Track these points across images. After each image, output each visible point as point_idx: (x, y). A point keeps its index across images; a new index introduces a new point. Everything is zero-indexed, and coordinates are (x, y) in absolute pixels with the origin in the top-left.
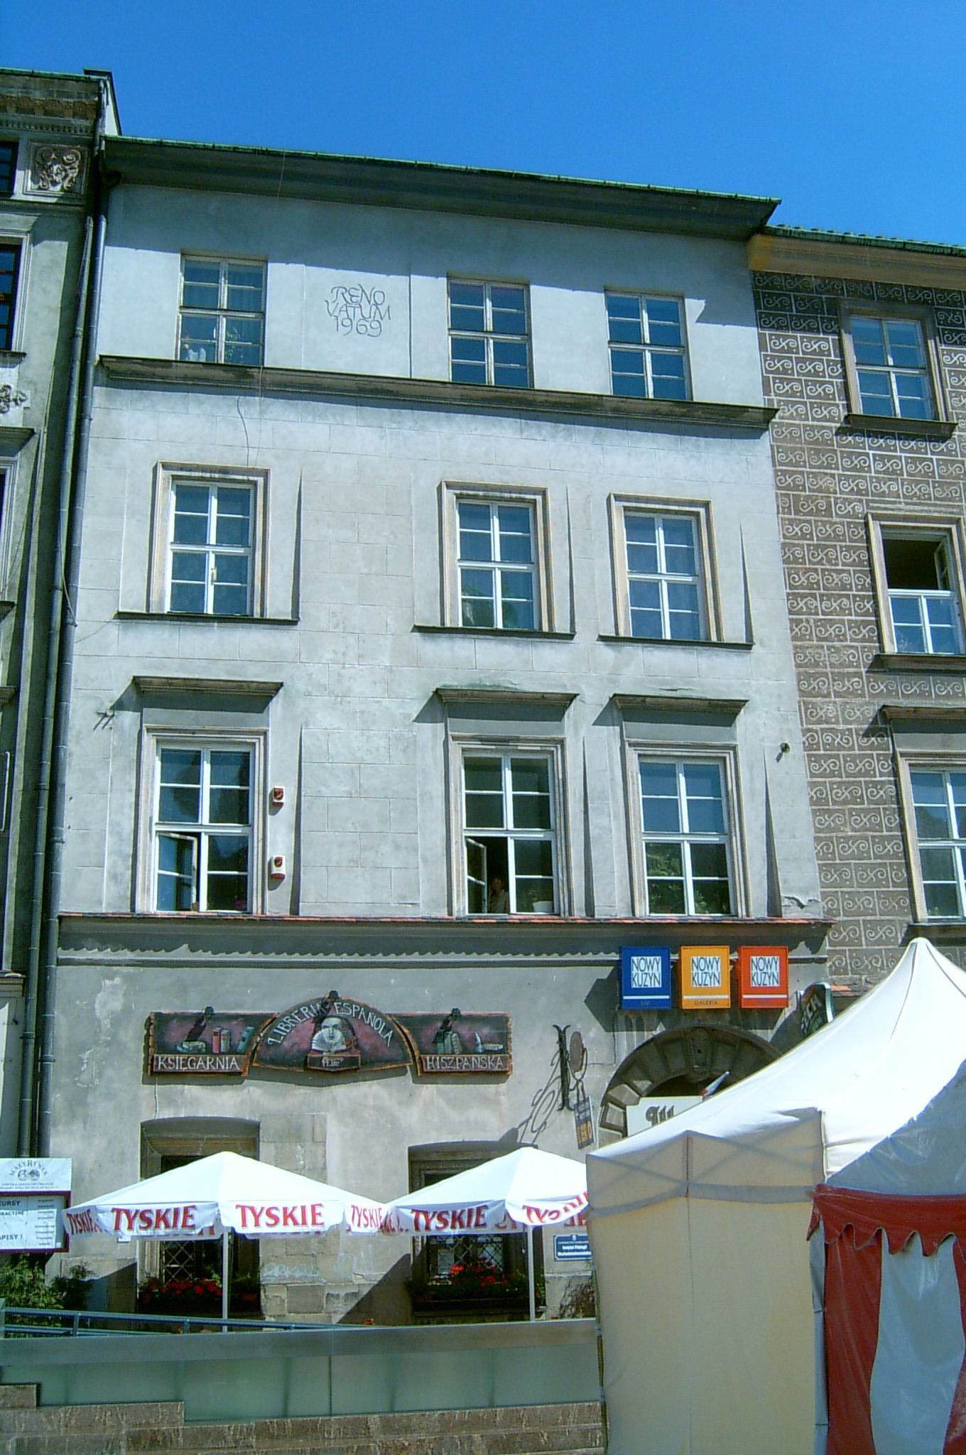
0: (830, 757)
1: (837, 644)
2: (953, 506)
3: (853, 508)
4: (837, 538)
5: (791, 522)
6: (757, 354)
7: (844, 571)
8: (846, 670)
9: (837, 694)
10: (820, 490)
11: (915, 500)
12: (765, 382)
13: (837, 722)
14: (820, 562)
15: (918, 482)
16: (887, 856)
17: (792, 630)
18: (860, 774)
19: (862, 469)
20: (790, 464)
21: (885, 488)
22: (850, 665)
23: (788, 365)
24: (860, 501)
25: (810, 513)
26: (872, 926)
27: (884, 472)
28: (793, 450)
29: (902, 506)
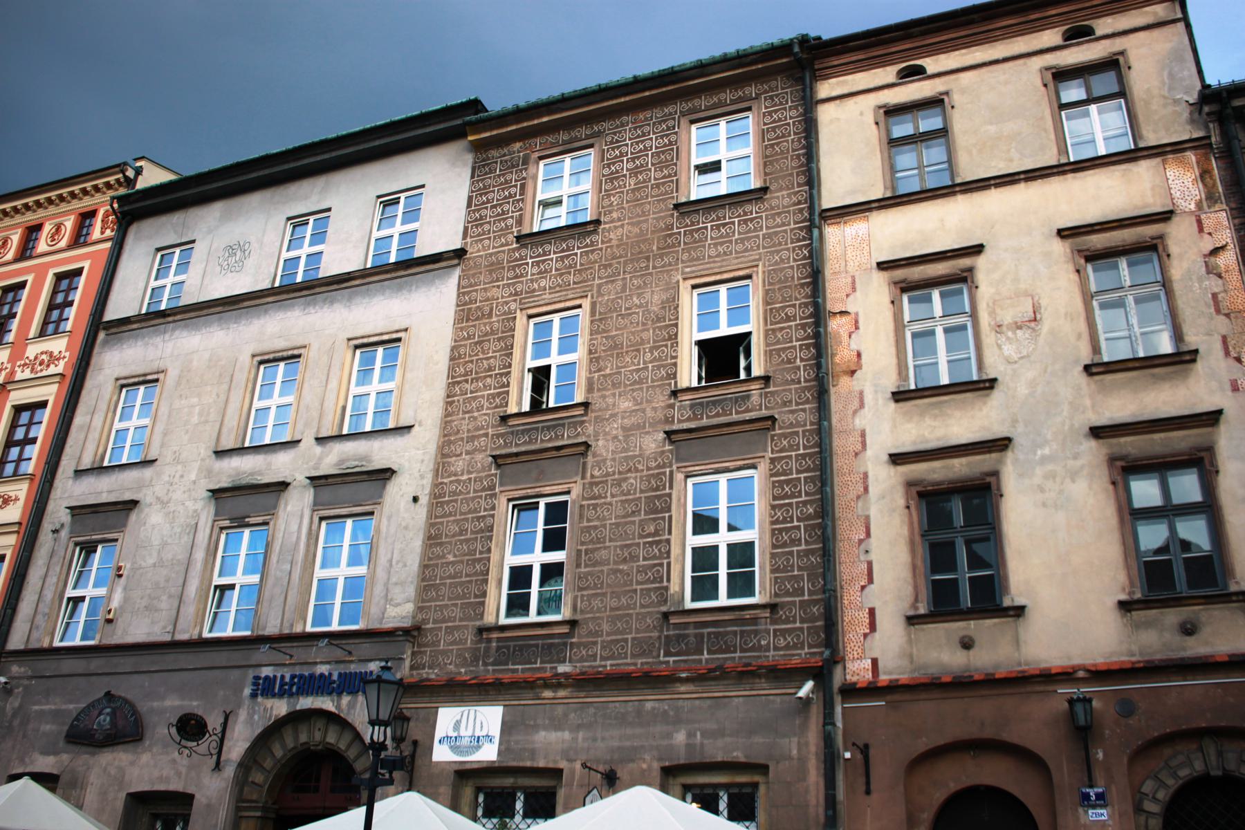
1: (476, 414)
4: (493, 332)
5: (462, 329)
6: (464, 211)
9: (468, 453)
12: (466, 229)
13: (462, 474)
14: (477, 355)
16: (476, 574)
18: (470, 512)
19: (522, 276)
20: (471, 286)
21: (536, 286)
23: (483, 212)
24: (515, 301)
25: (477, 319)
26: (450, 630)
28: (474, 275)
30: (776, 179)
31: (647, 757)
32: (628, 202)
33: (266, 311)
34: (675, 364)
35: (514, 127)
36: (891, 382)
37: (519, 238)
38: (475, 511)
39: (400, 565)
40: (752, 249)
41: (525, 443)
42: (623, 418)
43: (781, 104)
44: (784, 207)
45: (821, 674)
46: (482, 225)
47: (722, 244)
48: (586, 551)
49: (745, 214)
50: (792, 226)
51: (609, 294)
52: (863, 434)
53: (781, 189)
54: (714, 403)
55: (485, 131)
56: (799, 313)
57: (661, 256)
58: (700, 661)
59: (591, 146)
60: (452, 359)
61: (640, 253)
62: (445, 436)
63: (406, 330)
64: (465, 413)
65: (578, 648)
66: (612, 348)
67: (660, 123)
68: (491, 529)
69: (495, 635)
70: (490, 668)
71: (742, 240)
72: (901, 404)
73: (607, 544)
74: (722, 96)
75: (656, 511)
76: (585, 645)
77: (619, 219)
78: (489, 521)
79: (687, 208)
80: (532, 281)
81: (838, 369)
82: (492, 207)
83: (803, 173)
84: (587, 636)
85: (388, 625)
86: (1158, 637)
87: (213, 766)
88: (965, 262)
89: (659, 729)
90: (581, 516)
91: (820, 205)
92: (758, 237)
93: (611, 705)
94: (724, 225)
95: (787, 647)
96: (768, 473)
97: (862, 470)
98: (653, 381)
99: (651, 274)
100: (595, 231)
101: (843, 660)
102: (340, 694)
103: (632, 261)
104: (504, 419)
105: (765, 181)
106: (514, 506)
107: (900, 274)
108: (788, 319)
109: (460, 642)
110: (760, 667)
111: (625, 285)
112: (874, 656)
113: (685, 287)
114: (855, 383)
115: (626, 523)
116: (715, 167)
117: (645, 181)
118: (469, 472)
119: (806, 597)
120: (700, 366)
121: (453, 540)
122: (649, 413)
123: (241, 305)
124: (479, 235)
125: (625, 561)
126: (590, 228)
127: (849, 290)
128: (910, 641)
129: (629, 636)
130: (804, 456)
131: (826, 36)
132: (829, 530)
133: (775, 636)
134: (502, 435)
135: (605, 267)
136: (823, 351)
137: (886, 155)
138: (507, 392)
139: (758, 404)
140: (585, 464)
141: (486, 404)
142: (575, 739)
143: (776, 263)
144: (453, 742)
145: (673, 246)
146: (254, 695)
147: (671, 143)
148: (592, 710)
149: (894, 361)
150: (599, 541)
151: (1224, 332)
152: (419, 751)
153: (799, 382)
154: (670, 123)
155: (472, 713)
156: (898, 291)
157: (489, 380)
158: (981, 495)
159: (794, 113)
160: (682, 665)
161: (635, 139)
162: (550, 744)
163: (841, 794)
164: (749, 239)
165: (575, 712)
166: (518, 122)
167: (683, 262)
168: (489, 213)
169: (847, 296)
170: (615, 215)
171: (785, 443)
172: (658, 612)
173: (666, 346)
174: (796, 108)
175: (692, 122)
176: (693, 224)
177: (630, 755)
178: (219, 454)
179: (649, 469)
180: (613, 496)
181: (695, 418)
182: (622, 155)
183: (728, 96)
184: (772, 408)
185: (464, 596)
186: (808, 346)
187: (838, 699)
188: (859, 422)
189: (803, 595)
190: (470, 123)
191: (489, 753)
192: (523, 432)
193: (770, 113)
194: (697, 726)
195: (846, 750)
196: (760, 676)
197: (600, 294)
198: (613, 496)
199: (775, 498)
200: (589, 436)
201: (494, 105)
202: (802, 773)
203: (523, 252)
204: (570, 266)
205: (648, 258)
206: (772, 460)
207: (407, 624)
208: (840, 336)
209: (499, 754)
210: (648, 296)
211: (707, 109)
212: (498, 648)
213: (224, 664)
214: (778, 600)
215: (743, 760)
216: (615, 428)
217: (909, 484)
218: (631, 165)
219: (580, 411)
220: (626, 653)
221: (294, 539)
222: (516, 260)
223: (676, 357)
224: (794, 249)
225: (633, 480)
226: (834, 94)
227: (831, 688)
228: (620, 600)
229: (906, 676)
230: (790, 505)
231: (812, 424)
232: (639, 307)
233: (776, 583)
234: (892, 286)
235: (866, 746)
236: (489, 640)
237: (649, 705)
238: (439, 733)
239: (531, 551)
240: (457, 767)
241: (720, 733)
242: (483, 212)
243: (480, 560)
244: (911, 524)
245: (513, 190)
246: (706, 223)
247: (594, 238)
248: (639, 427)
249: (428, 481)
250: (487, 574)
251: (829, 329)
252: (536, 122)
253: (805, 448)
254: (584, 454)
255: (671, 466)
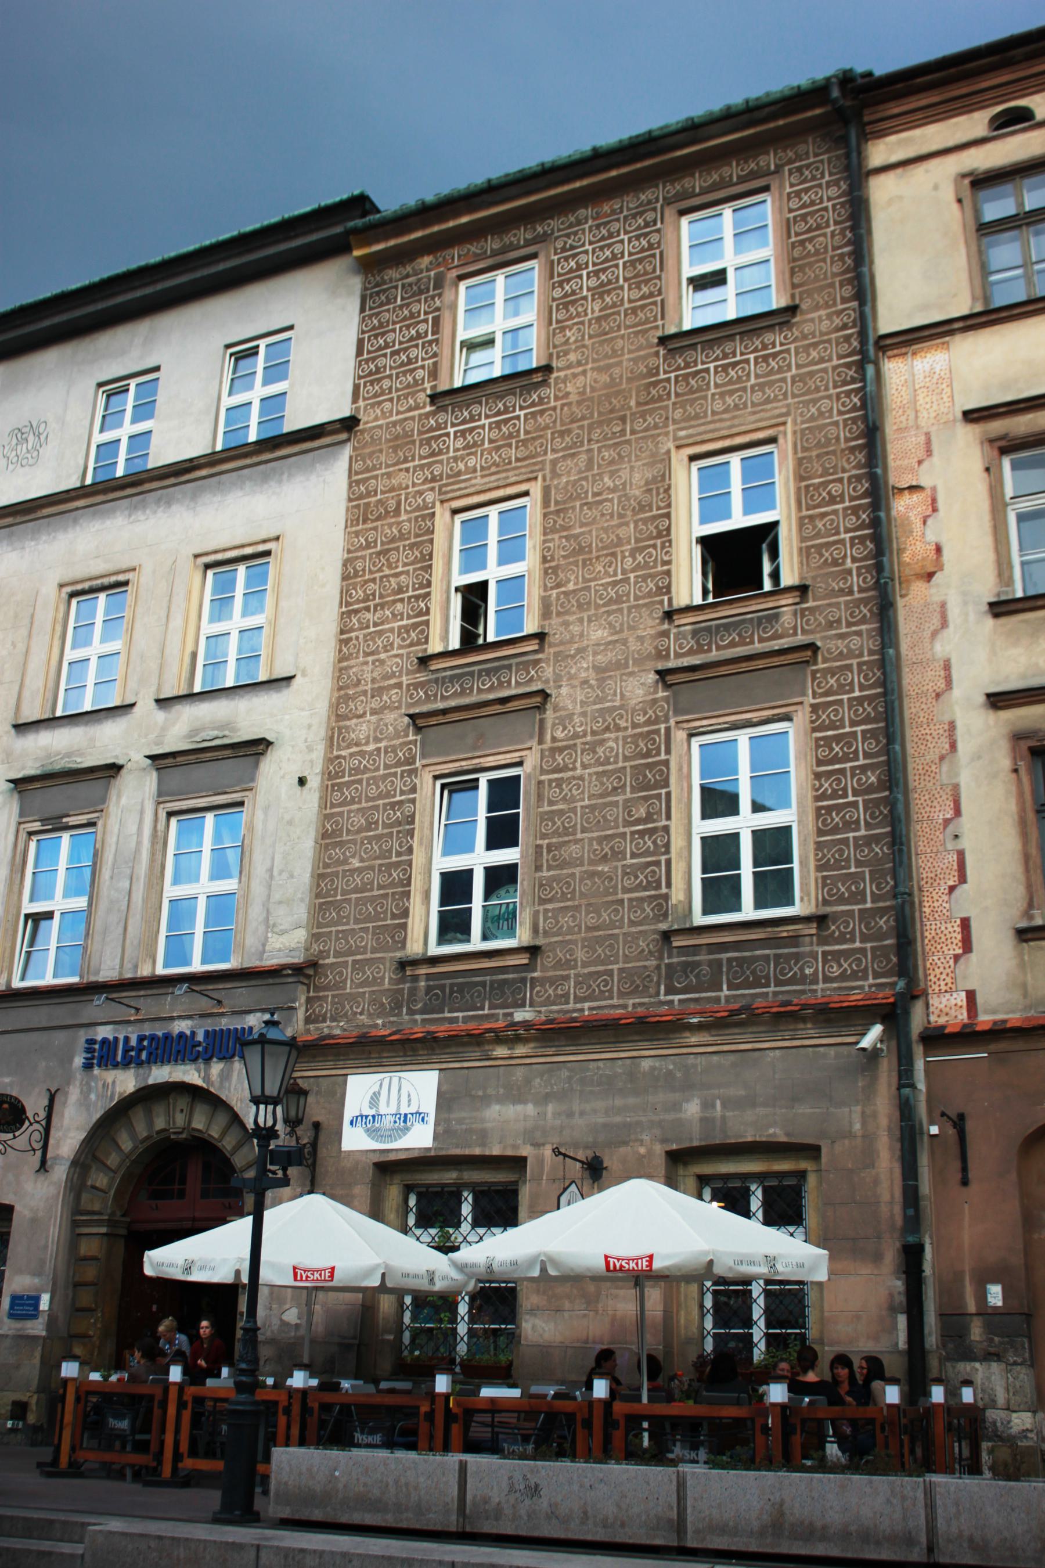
0: (353, 782)
1: (383, 656)
2: (534, 464)
3: (424, 500)
4: (402, 537)
5: (357, 534)
7: (401, 573)
8: (387, 683)
9: (374, 712)
10: (392, 489)
11: (493, 469)
12: (356, 388)
13: (367, 743)
14: (380, 570)
15: (498, 449)
16: (392, 885)
17: (340, 651)
18: (380, 796)
19: (440, 452)
20: (368, 470)
21: (461, 466)
22: (393, 675)
23: (381, 362)
24: (432, 489)
25: (378, 519)
27: (464, 448)
29: (478, 481)
30: (809, 293)
31: (646, 1138)
32: (590, 337)
33: (75, 521)
34: (668, 573)
35: (419, 234)
36: (987, 589)
37: (434, 398)
38: (388, 795)
39: (285, 875)
40: (776, 399)
41: (455, 693)
42: (595, 654)
43: (814, 178)
44: (822, 334)
45: (893, 1015)
46: (379, 380)
47: (731, 393)
48: (549, 846)
49: (765, 347)
50: (835, 362)
51: (569, 473)
52: (947, 666)
53: (817, 308)
54: (726, 627)
55: (378, 241)
56: (848, 490)
57: (643, 415)
58: (718, 1000)
59: (534, 256)
60: (345, 578)
61: (612, 411)
62: (340, 689)
63: (277, 538)
64: (367, 654)
65: (542, 985)
66: (574, 553)
67: (634, 216)
68: (411, 819)
69: (423, 971)
70: (418, 1017)
71: (761, 387)
72: (1003, 620)
73: (579, 836)
74: (726, 171)
75: (647, 787)
76: (553, 981)
77: (579, 363)
78: (408, 808)
79: (678, 343)
80: (456, 459)
81: (908, 571)
82: (393, 354)
83: (849, 281)
84: (554, 968)
85: (271, 961)
87: (37, 1165)
89: (661, 1097)
90: (540, 797)
91: (875, 329)
92: (784, 380)
93: (592, 1065)
94: (734, 365)
95: (843, 977)
96: (809, 726)
97: (947, 718)
98: (637, 598)
99: (628, 442)
100: (544, 383)
101: (925, 993)
102: (208, 1060)
103: (600, 423)
104: (424, 661)
105: (793, 296)
106: (443, 787)
107: (997, 427)
108: (833, 500)
109: (375, 981)
110: (805, 1006)
111: (590, 460)
112: (970, 988)
113: (679, 459)
114: (933, 591)
115: (606, 805)
116: (717, 278)
117: (614, 305)
118: (377, 740)
119: (869, 905)
120: (704, 574)
121: (358, 837)
122: (633, 645)
123: (39, 514)
124: (375, 396)
125: (604, 859)
126: (538, 378)
127: (921, 454)
128: (1022, 965)
129: (615, 967)
130: (860, 700)
131: (879, 71)
132: (900, 807)
133: (825, 961)
134: (422, 685)
135: (562, 434)
136: (886, 545)
137: (974, 248)
138: (427, 623)
139: (790, 626)
140: (542, 722)
141: (397, 641)
142: (542, 1115)
143: (812, 418)
144: (369, 1122)
145: (660, 399)
146: (88, 1066)
147: (651, 247)
148: (565, 1074)
149: (991, 556)
150: (566, 832)
152: (322, 1138)
153: (851, 592)
154: (650, 216)
155: (395, 1080)
156: (996, 453)
157: (399, 606)
159: (833, 191)
160: (692, 1006)
161: (600, 243)
162: (506, 1122)
163: (925, 1187)
164: (771, 384)
165: (542, 1076)
166: (425, 225)
167: (675, 422)
168: (389, 362)
169: (920, 462)
170: (572, 357)
171: (832, 681)
172: (655, 932)
173: (654, 546)
174: (836, 183)
175: (682, 213)
176: (687, 365)
177: (622, 1135)
178: (21, 728)
179: (635, 726)
180: (584, 766)
181: (700, 650)
182: (579, 267)
183: (734, 170)
184: (812, 632)
185: (377, 918)
186: (862, 539)
187: (918, 1050)
188: (941, 648)
189: (865, 902)
190: (355, 231)
191: (420, 1138)
192: (452, 678)
193: (798, 194)
194: (716, 1092)
195: (932, 1123)
196: (804, 1020)
197: (555, 474)
198: (584, 766)
199: (820, 763)
200: (547, 681)
201: (390, 201)
202: (869, 1157)
203: (442, 417)
204: (511, 436)
205: (623, 419)
206: (815, 708)
207: (298, 959)
208: (910, 523)
209: (435, 1139)
210: (624, 474)
211: (704, 191)
212: (429, 989)
213: (44, 1024)
214: (828, 909)
215: (783, 1139)
216: (583, 669)
217: (1017, 737)
218: (593, 282)
219: (532, 645)
220: (611, 991)
221: (133, 844)
222: (432, 429)
223: (669, 563)
224: (838, 395)
225: (613, 743)
226: (894, 158)
227: (907, 1034)
228: (600, 916)
229: (1017, 1015)
230: (842, 771)
231: (871, 653)
232: (613, 490)
233: (824, 885)
234: (986, 446)
235: (961, 1117)
236: (415, 978)
237: (646, 1064)
238: (349, 1114)
239: (470, 849)
240: (377, 1158)
241: (750, 1102)
242: (381, 362)
243: (397, 864)
244: (1021, 794)
245: (422, 327)
246: (707, 363)
247: (544, 392)
248: (619, 665)
249: (319, 754)
250: (409, 884)
251: (894, 513)
252: (451, 224)
253: (862, 688)
254: (540, 708)
255: (667, 720)
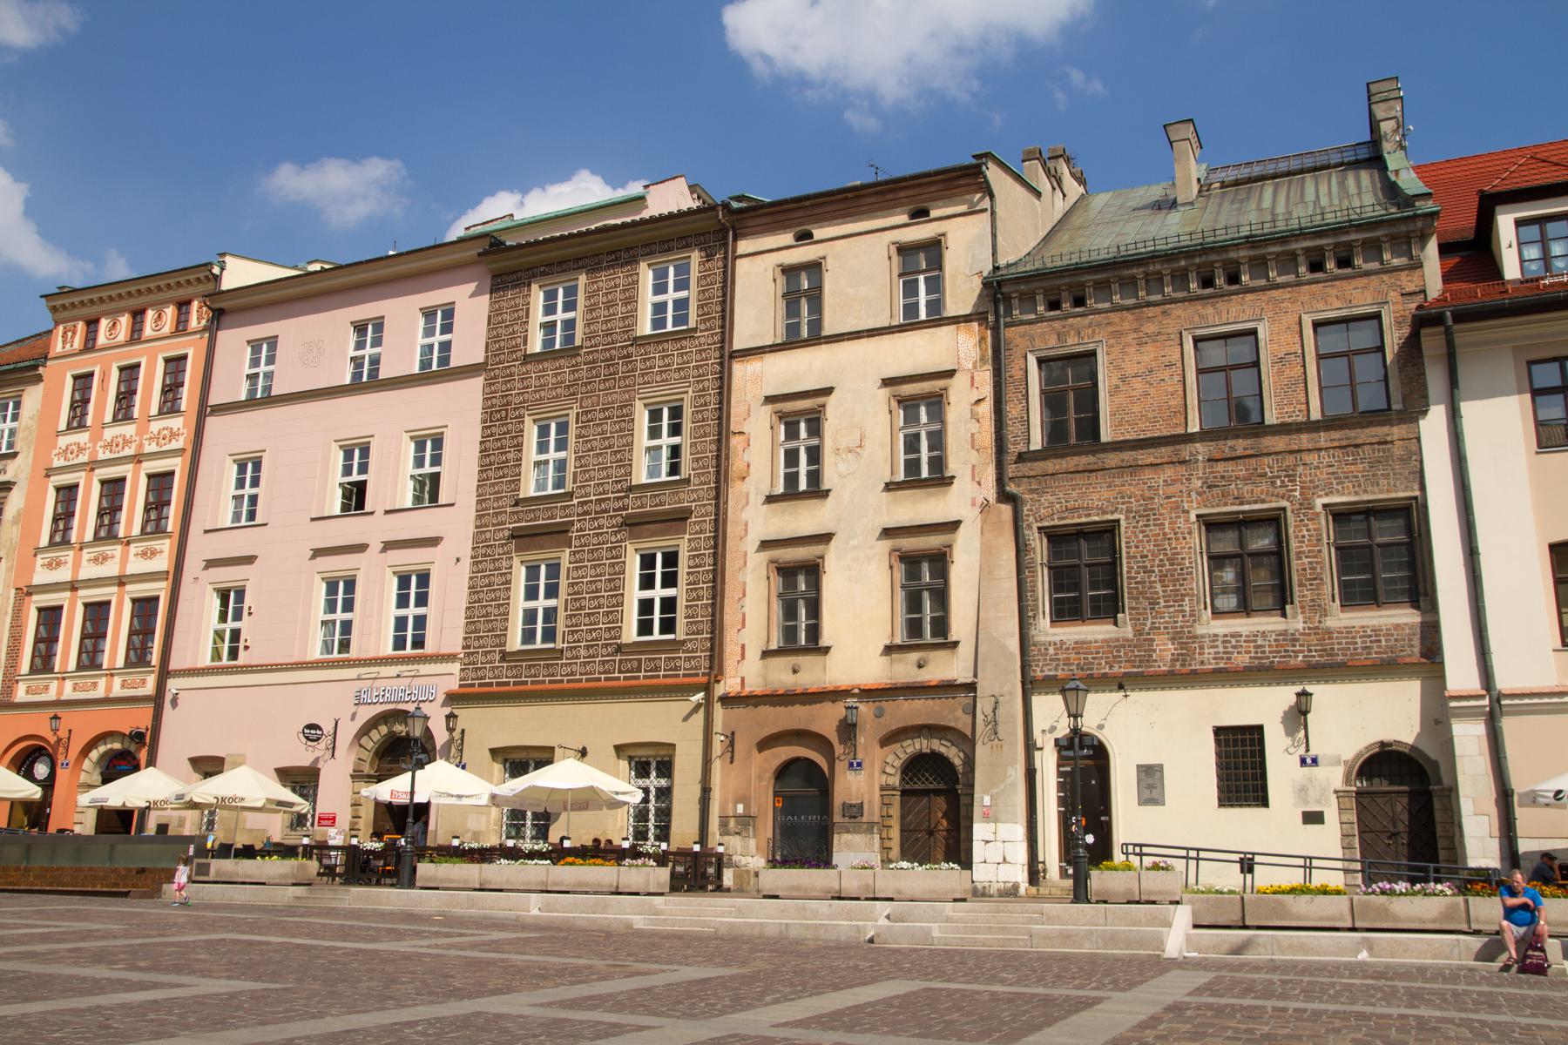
45: (707, 688)
86: (905, 670)
88: (820, 400)
151: (974, 461)
158: (813, 570)
187: (718, 707)
